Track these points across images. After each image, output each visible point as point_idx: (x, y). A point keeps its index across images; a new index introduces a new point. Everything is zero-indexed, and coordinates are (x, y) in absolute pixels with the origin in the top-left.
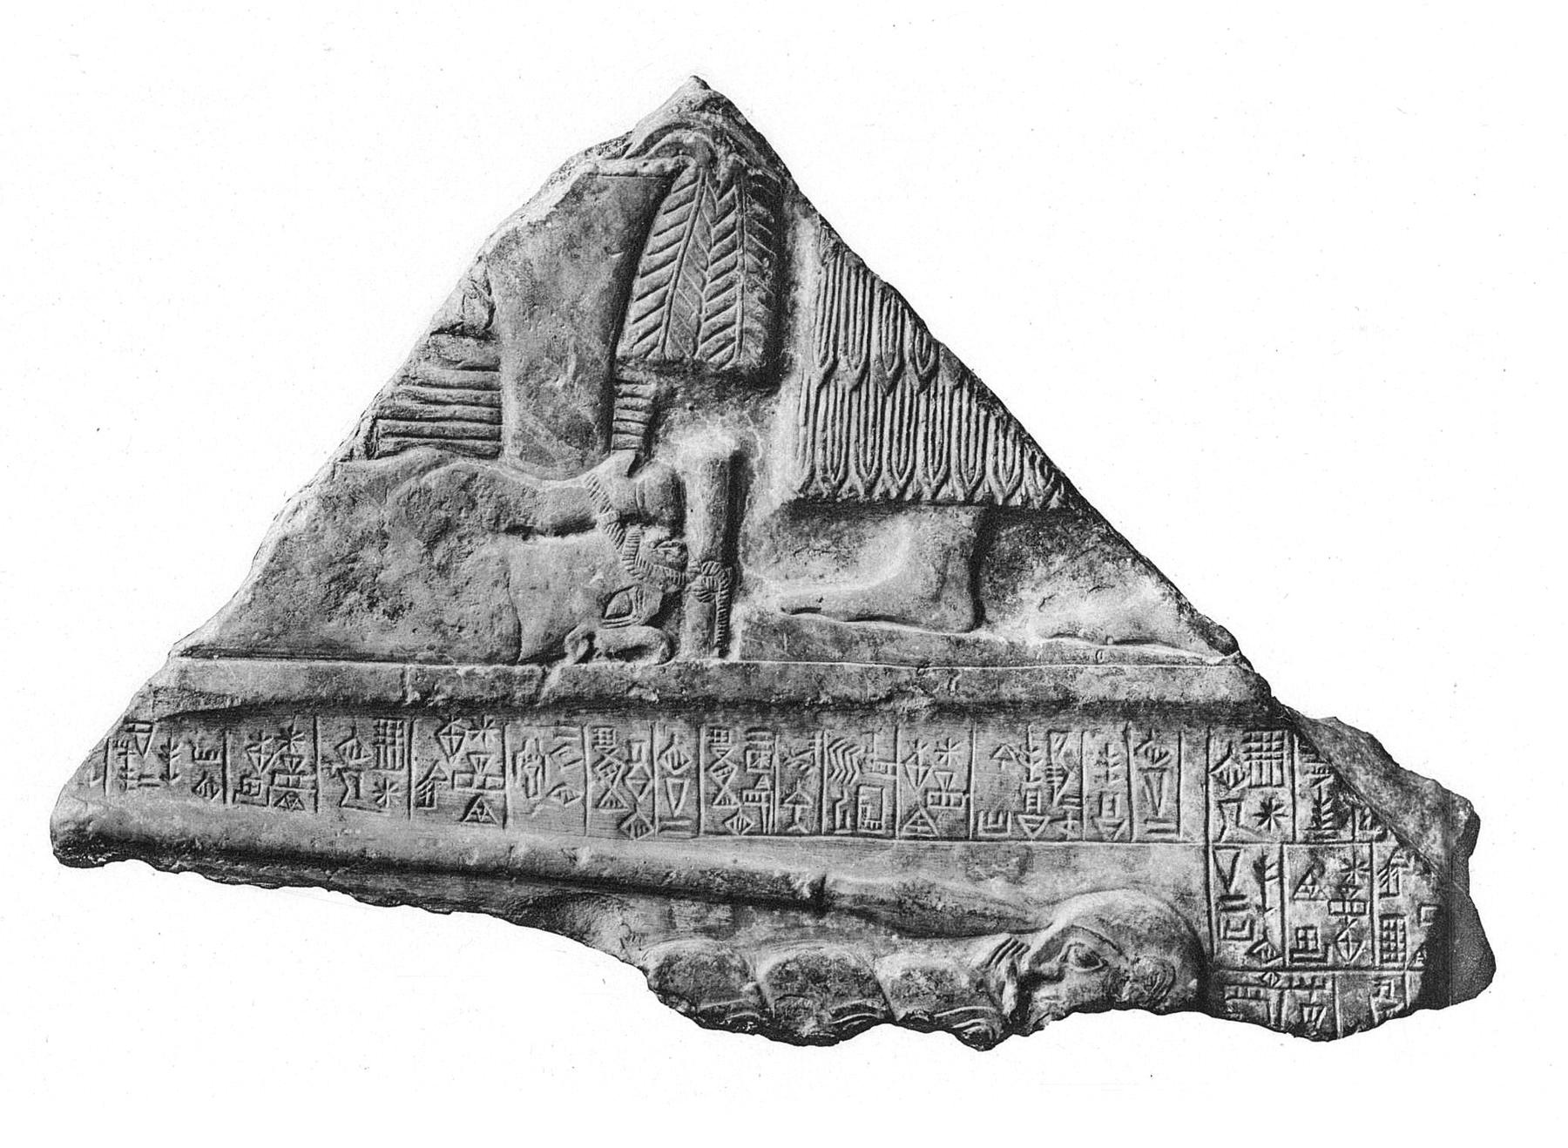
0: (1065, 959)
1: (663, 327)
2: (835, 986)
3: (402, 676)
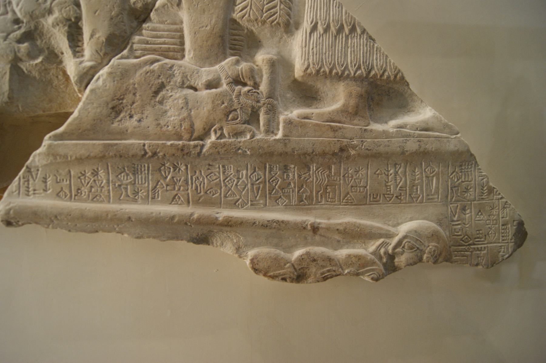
0: (403, 247)
1: (249, 7)
2: (321, 263)
3: (144, 145)
